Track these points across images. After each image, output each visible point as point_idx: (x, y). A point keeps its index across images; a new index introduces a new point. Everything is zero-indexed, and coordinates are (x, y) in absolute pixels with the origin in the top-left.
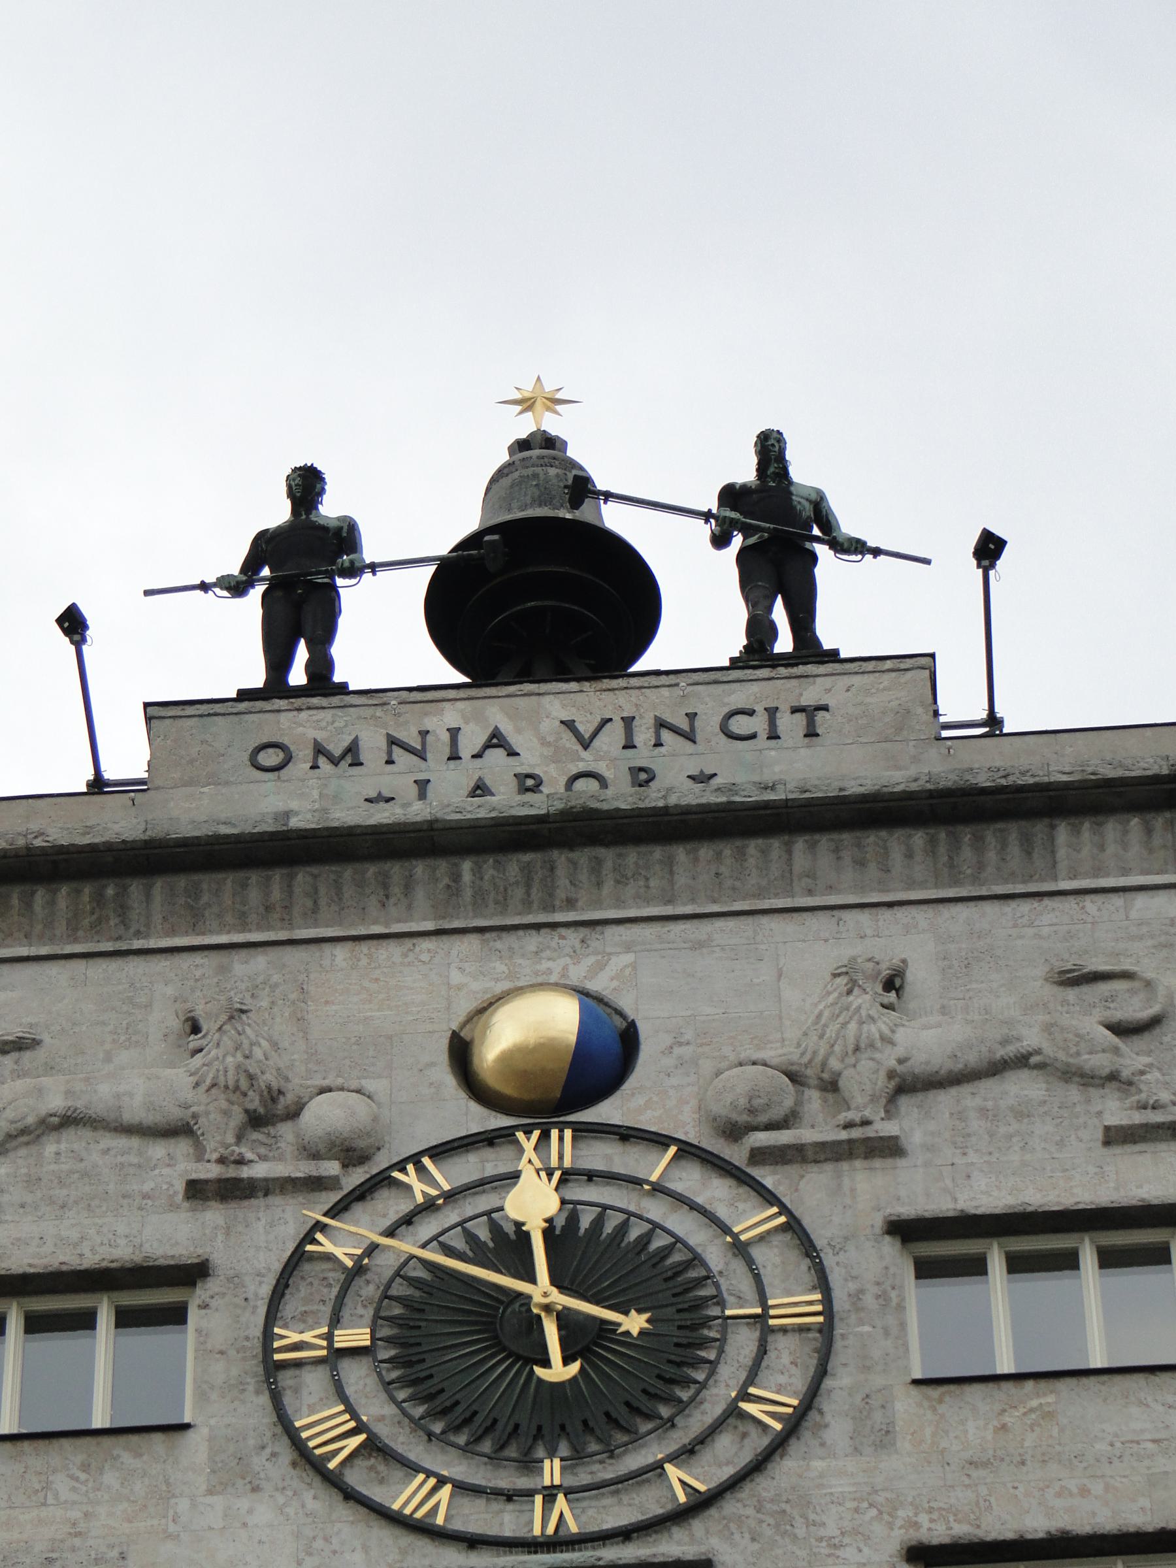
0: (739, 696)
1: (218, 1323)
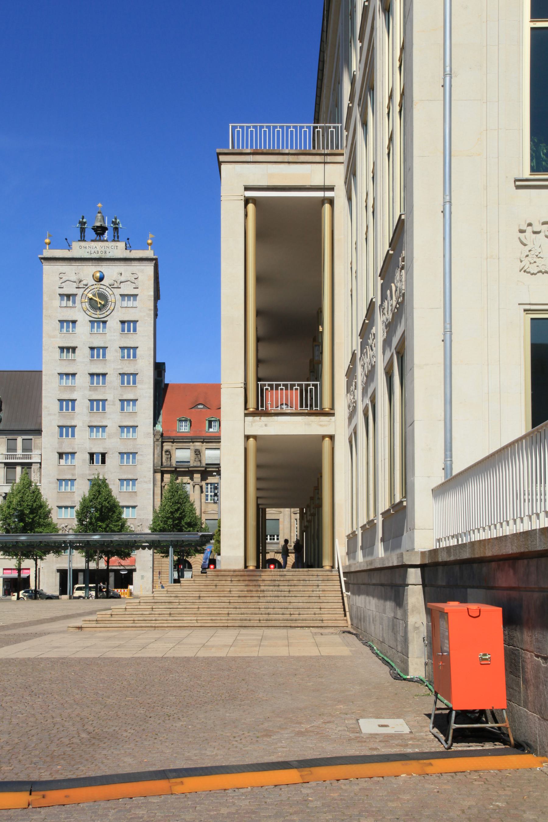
1: (78, 298)
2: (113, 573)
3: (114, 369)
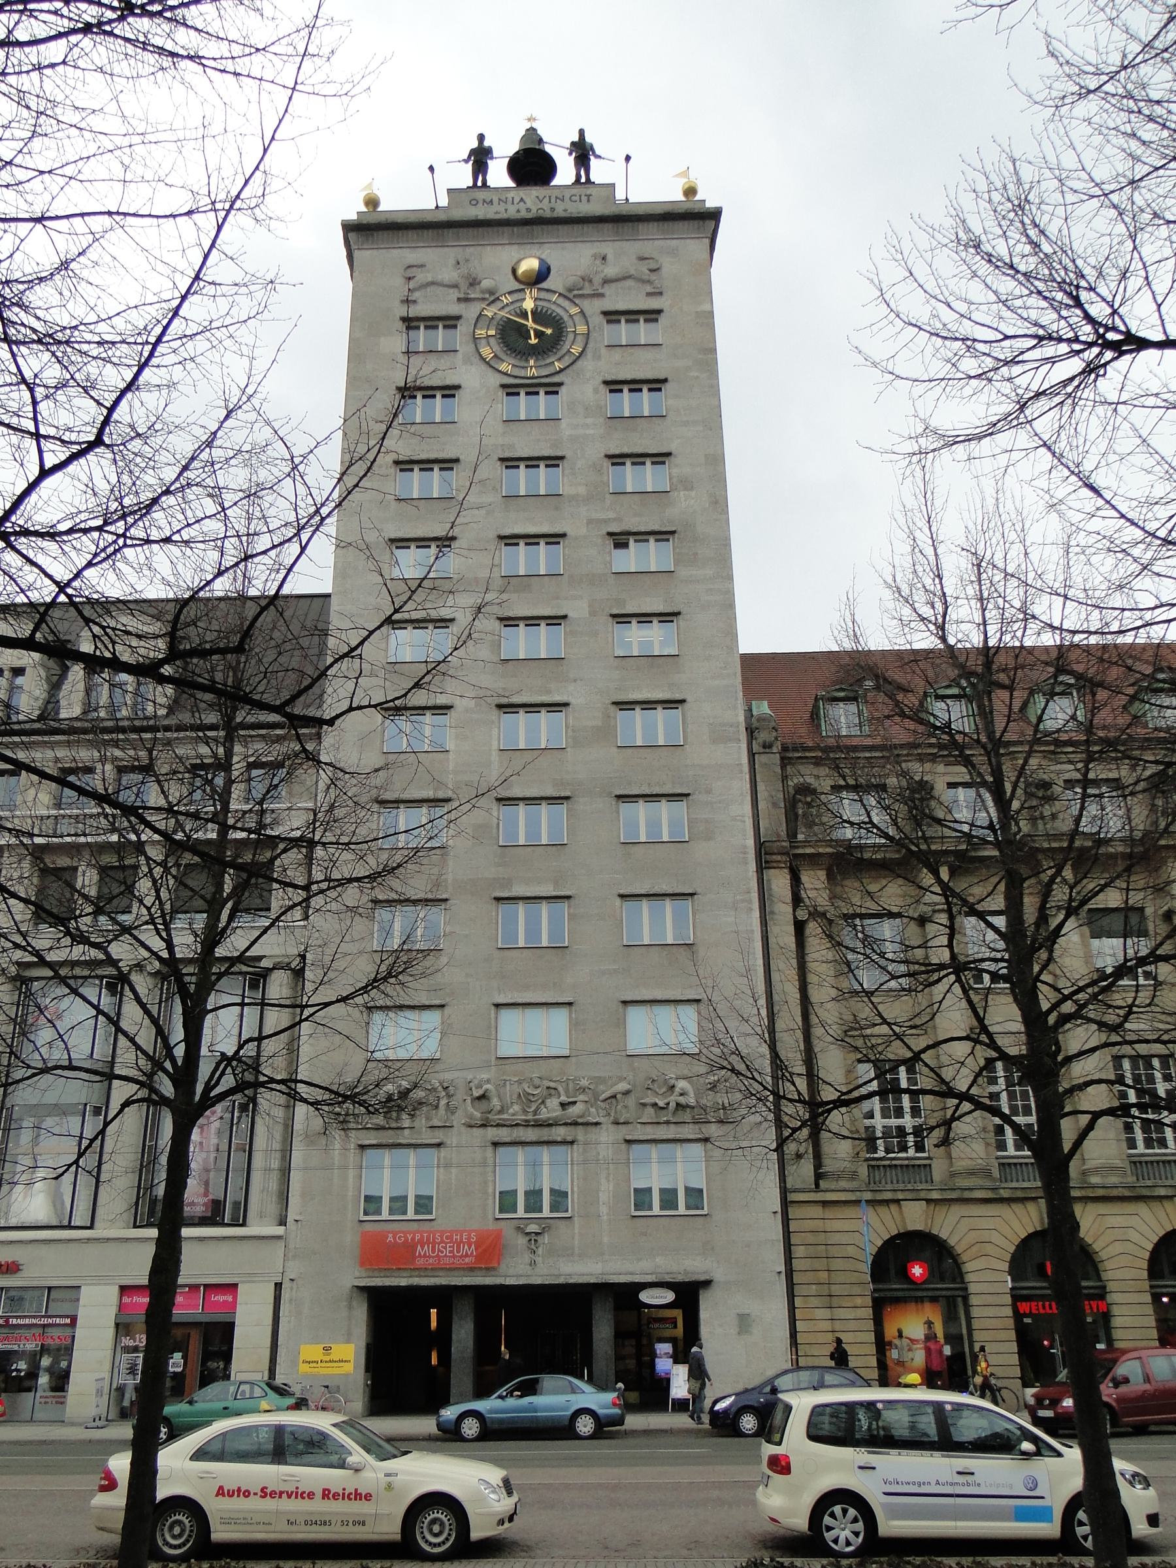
0: (574, 191)
1: (463, 328)
2: (610, 1304)
3: (590, 522)
